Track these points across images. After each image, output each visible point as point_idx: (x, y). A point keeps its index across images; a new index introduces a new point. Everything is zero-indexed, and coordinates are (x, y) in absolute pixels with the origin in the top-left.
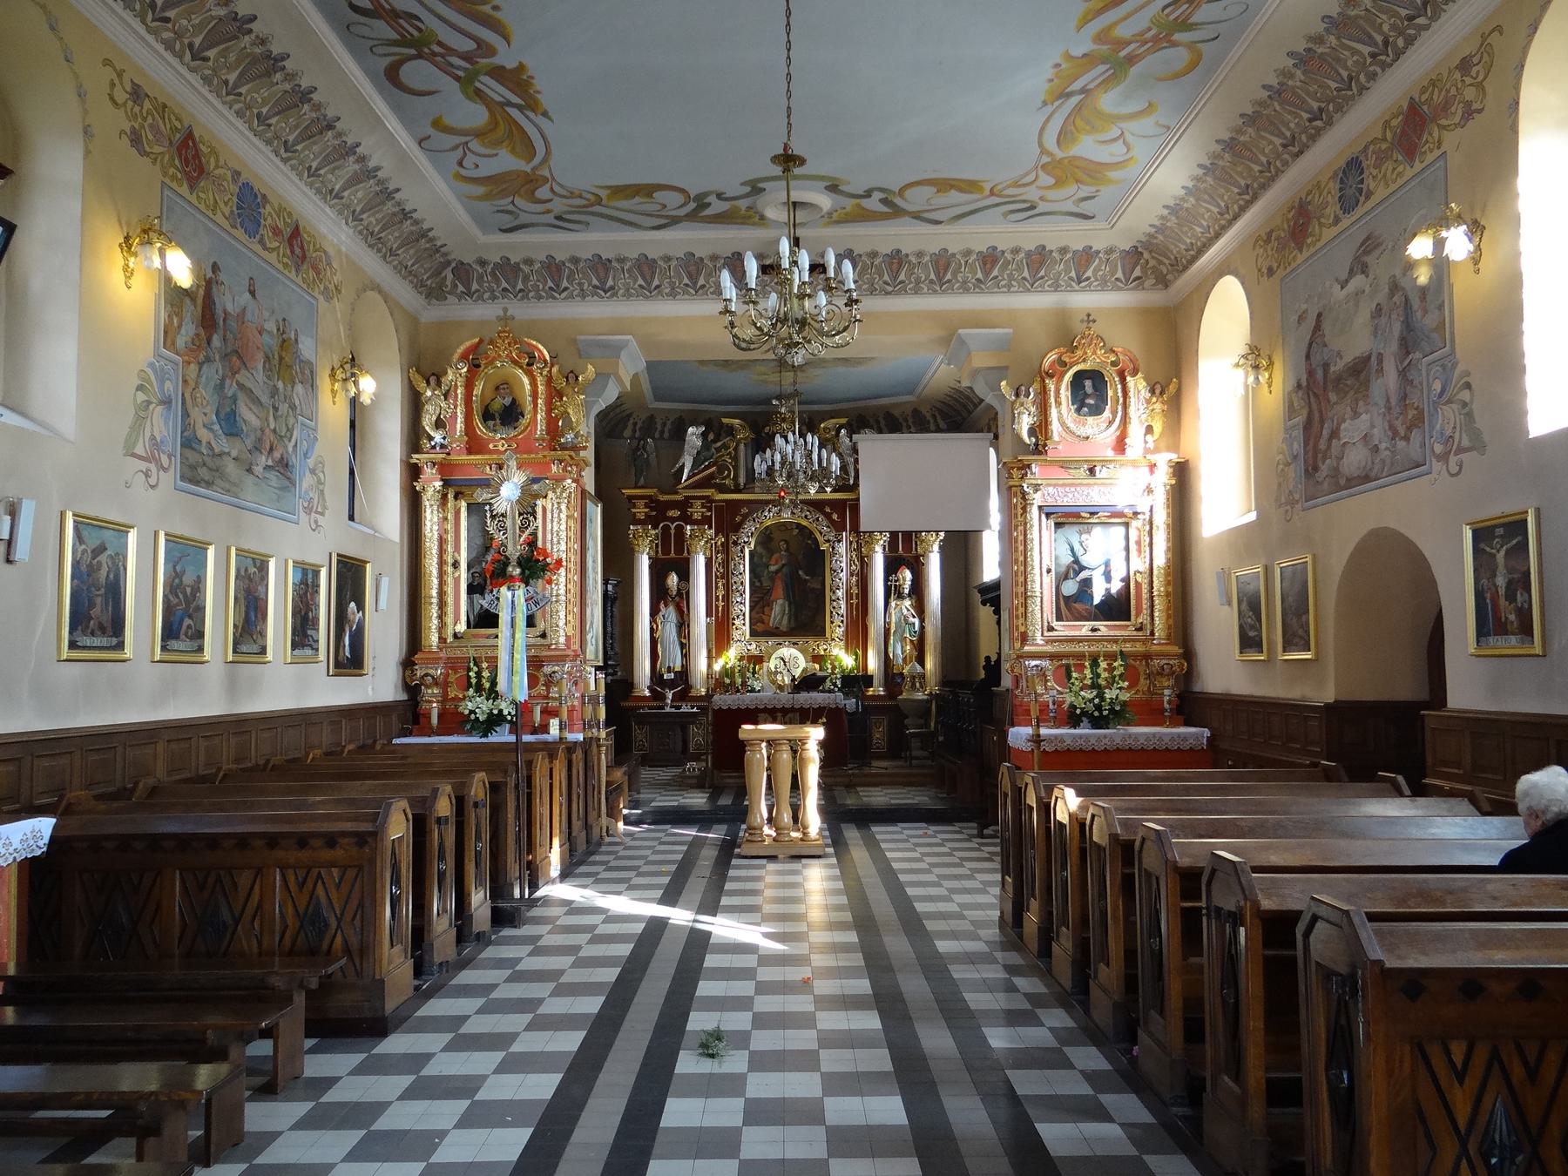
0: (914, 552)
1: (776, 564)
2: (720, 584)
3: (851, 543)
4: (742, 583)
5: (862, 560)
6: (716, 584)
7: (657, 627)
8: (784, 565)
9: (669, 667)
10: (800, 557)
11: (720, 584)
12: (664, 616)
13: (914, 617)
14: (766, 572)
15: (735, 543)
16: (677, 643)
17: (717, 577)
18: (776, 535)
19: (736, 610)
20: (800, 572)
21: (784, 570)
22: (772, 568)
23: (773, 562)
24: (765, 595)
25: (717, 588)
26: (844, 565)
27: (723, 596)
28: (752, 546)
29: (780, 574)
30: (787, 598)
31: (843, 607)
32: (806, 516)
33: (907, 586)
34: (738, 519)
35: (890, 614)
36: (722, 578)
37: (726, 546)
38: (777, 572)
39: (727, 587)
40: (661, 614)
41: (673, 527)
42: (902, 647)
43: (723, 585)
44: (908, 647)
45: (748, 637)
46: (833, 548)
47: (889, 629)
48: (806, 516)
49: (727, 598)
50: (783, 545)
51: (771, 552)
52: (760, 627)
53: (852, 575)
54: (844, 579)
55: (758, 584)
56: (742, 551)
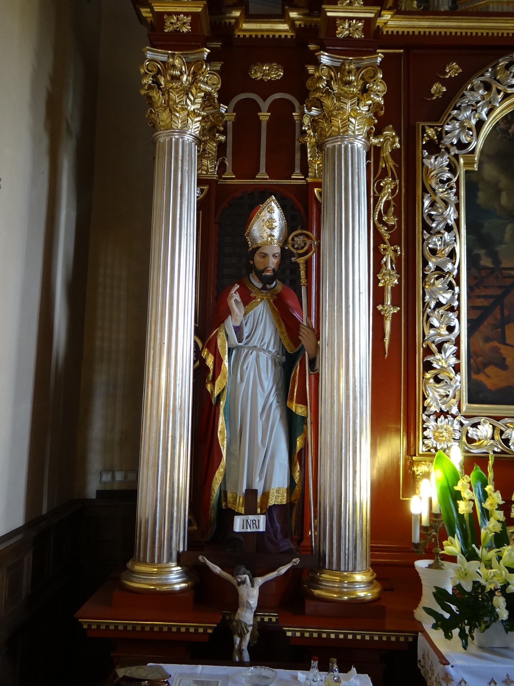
7: (218, 361)
9: (251, 493)
11: (387, 259)
12: (238, 330)
16: (276, 414)
27: (396, 290)
40: (230, 323)
41: (265, 105)
43: (397, 261)
55: (486, 262)
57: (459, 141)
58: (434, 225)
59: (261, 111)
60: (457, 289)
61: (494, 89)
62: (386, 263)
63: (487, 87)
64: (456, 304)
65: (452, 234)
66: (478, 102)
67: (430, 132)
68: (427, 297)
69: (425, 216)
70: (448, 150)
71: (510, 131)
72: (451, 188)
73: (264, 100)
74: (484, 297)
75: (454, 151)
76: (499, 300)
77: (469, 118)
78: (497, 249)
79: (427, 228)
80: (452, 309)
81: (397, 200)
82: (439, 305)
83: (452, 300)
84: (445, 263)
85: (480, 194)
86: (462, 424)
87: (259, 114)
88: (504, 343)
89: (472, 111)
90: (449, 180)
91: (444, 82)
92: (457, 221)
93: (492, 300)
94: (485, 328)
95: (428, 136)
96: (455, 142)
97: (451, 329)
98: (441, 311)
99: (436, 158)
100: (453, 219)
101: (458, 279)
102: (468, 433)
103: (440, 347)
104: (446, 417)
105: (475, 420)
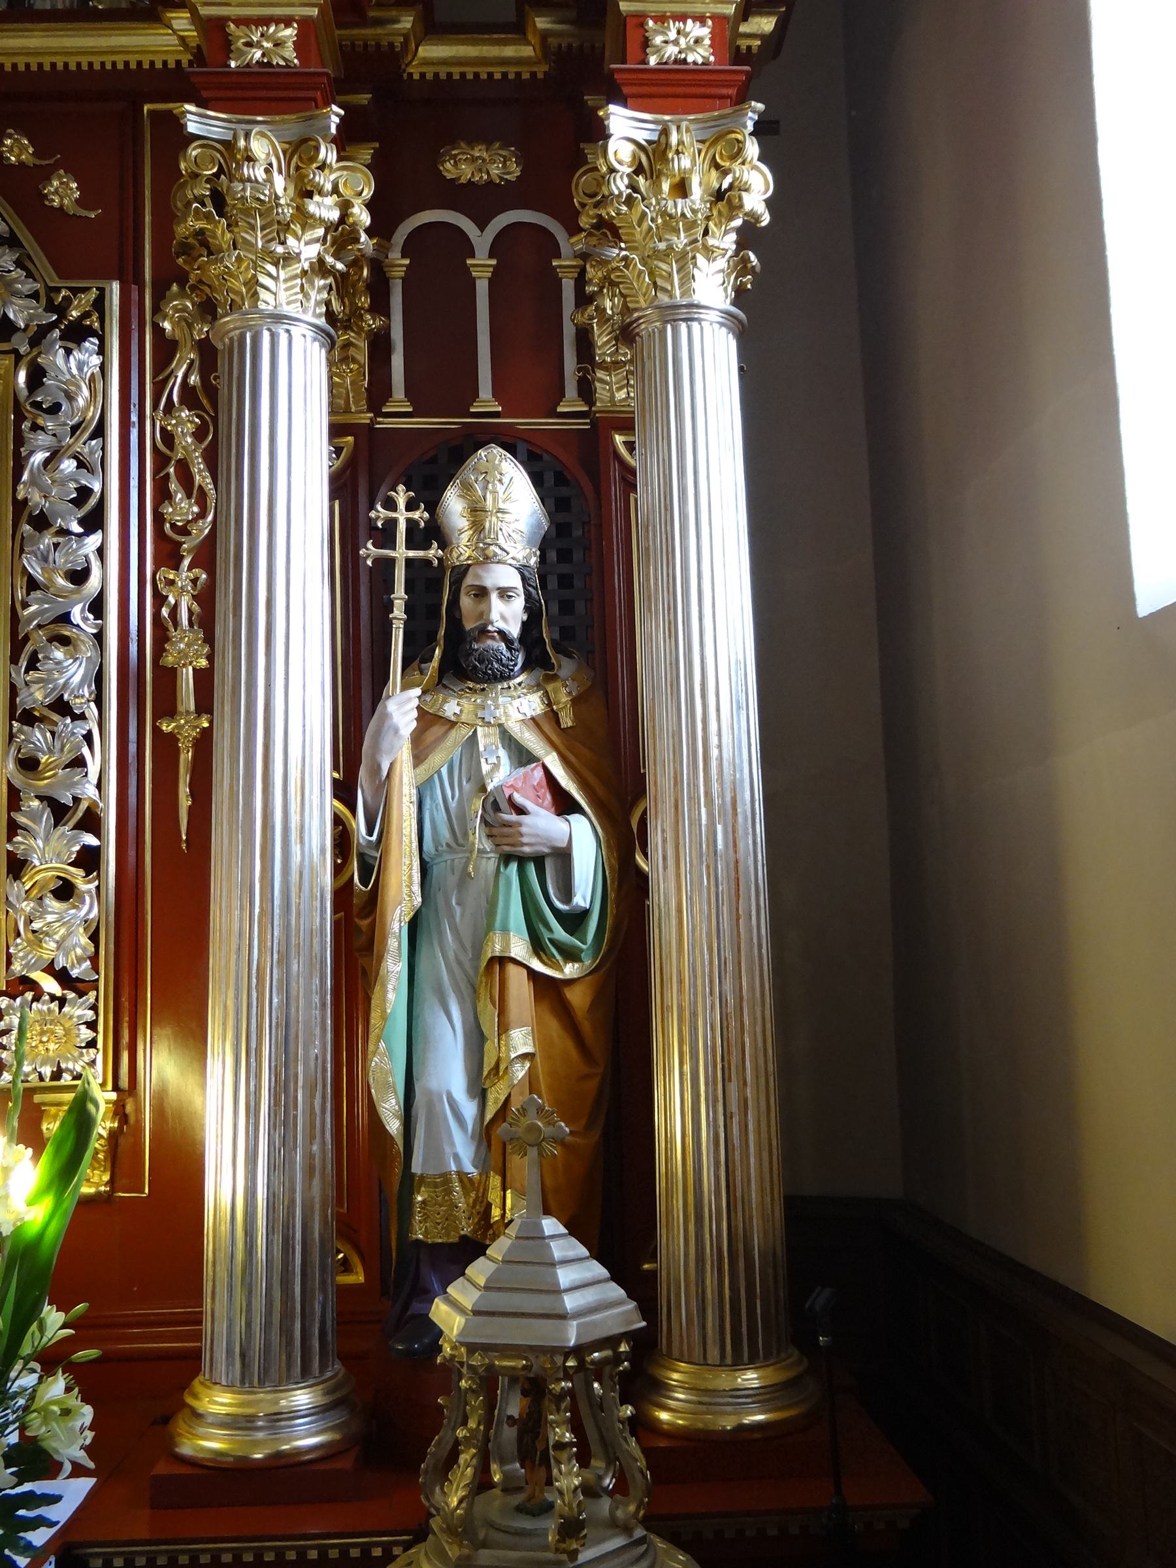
0: (571, 403)
3: (166, 349)
13: (564, 805)
33: (505, 576)
35: (384, 786)
42: (476, 1041)
44: (521, 1041)
46: (37, 376)
47: (373, 901)
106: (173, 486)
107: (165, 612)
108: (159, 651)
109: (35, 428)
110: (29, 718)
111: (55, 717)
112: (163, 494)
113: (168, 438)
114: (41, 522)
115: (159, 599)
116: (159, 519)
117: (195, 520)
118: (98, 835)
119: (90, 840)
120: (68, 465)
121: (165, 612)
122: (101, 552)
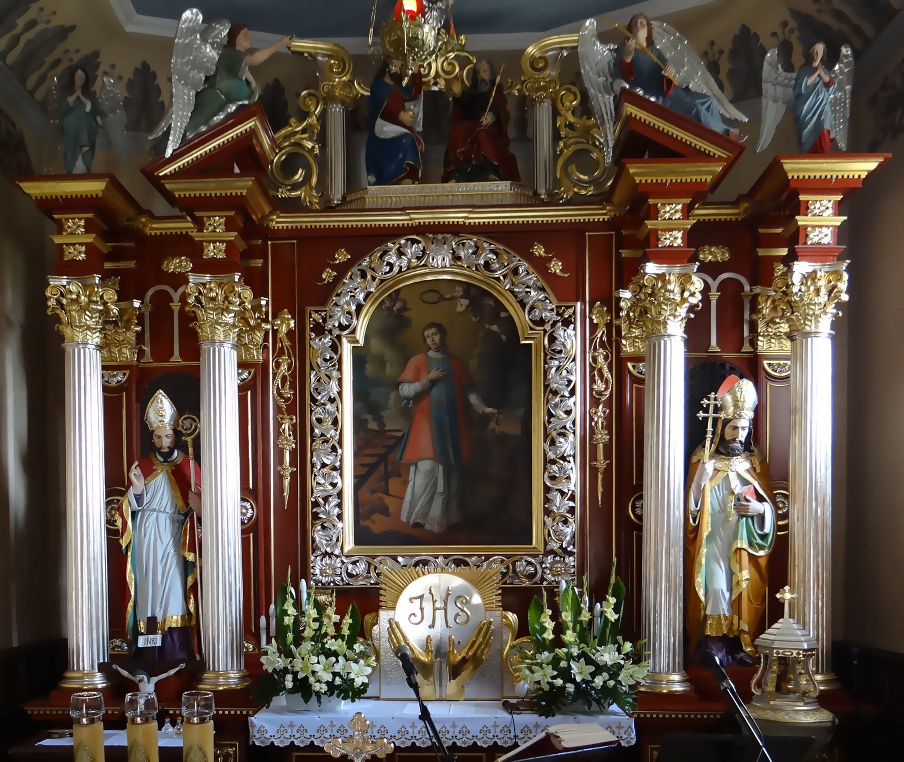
1: (416, 379)
2: (286, 426)
4: (335, 422)
5: (619, 364)
6: (278, 424)
8: (433, 383)
10: (473, 364)
11: (286, 426)
14: (393, 395)
15: (320, 330)
17: (278, 409)
18: (418, 314)
19: (319, 486)
20: (473, 399)
21: (435, 392)
22: (408, 389)
23: (409, 373)
24: (390, 449)
25: (278, 434)
26: (576, 378)
27: (293, 453)
28: (360, 335)
29: (425, 403)
30: (441, 456)
31: (575, 476)
32: (487, 265)
34: (328, 275)
36: (291, 411)
37: (298, 338)
38: (419, 397)
39: (301, 432)
43: (294, 427)
45: (349, 544)
46: (553, 339)
48: (487, 265)
49: (300, 457)
50: (432, 337)
51: (405, 355)
52: (378, 523)
53: (595, 403)
54: (577, 413)
55: (373, 425)
56: (335, 347)
57: (340, 324)
58: (319, 398)
59: (173, 302)
60: (339, 451)
61: (369, 277)
62: (284, 430)
63: (364, 275)
64: (338, 464)
65: (334, 405)
66: (355, 289)
67: (315, 316)
68: (314, 459)
69: (312, 390)
70: (330, 332)
71: (395, 309)
72: (334, 365)
73: (176, 291)
74: (371, 455)
75: (336, 332)
76: (383, 458)
77: (348, 303)
78: (382, 414)
79: (314, 400)
80: (334, 469)
81: (293, 375)
82: (324, 465)
83: (335, 461)
84: (328, 430)
85: (368, 366)
86: (343, 563)
87: (171, 304)
88: (388, 494)
89: (351, 296)
90: (331, 358)
91: (334, 267)
92: (340, 393)
93: (377, 458)
94: (372, 482)
95: (314, 320)
96: (337, 325)
97: (334, 485)
98: (325, 470)
99: (320, 340)
100: (335, 392)
101: (340, 442)
102: (347, 569)
103: (326, 499)
104: (330, 557)
105: (354, 559)
106: (597, 377)
107: (593, 424)
108: (591, 438)
109: (552, 358)
110: (553, 462)
111: (562, 462)
112: (593, 381)
113: (595, 359)
114: (555, 393)
115: (592, 419)
116: (592, 389)
117: (604, 391)
118: (575, 503)
119: (571, 504)
120: (564, 373)
121: (593, 424)
122: (574, 403)
